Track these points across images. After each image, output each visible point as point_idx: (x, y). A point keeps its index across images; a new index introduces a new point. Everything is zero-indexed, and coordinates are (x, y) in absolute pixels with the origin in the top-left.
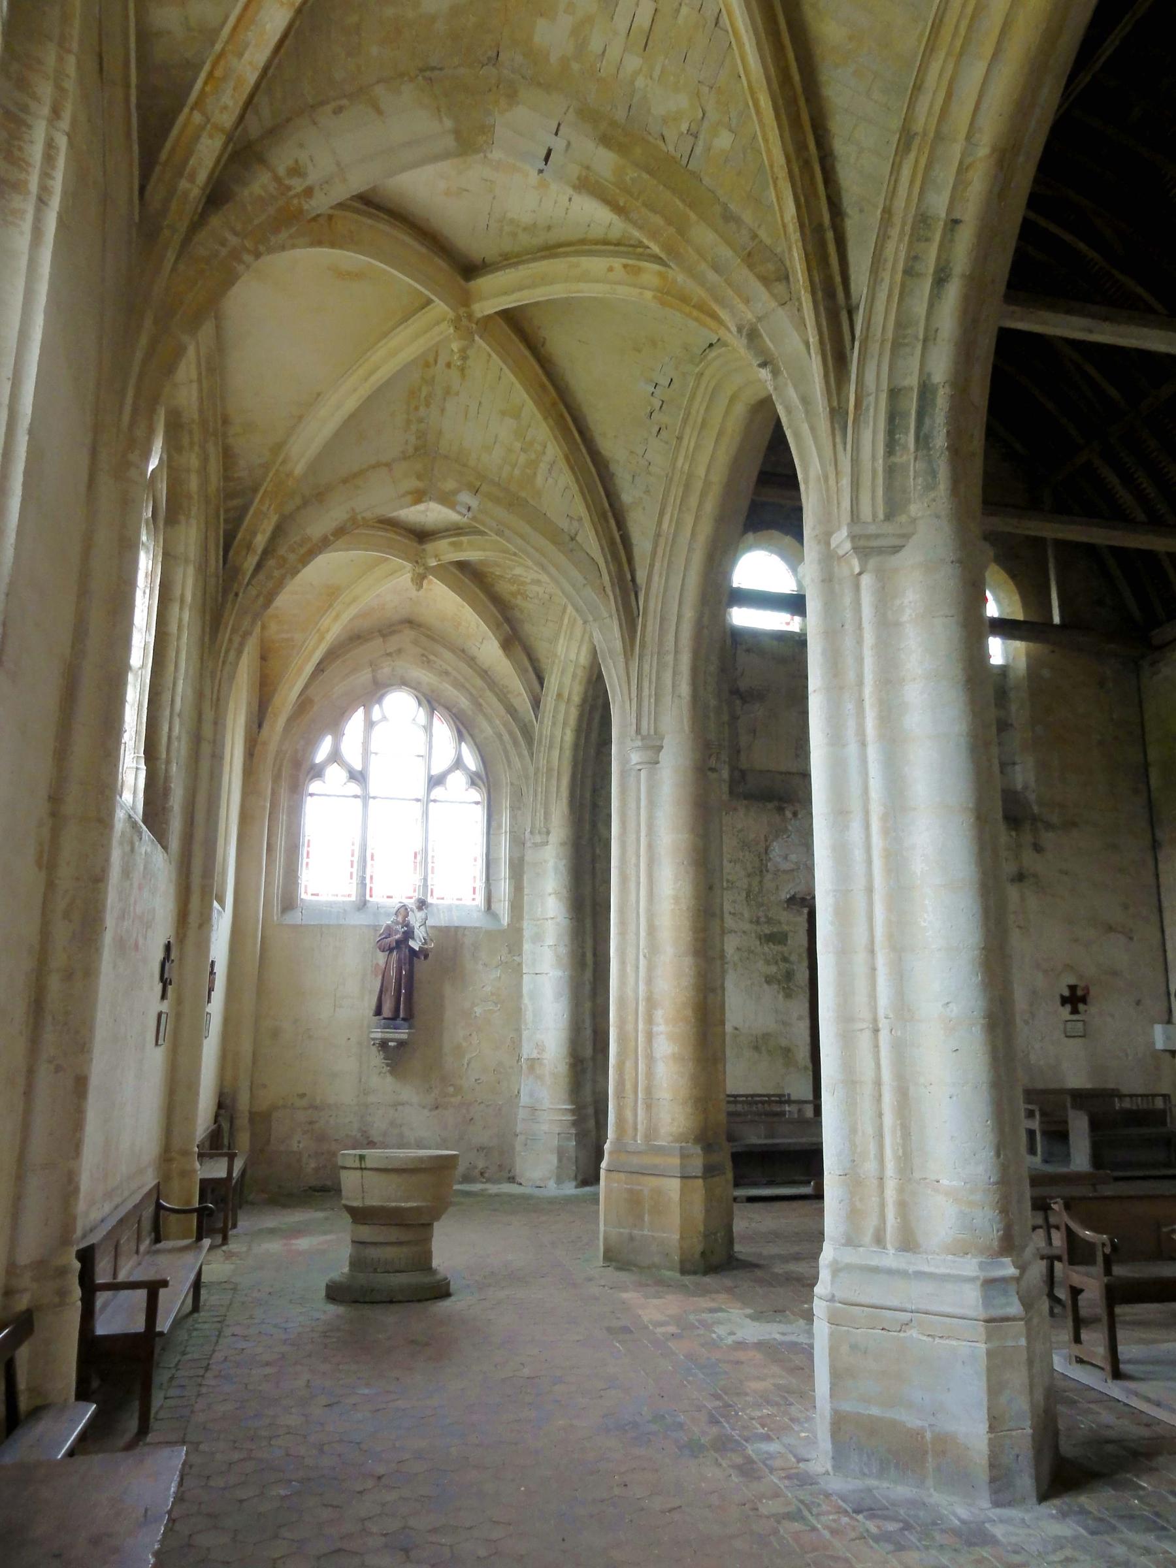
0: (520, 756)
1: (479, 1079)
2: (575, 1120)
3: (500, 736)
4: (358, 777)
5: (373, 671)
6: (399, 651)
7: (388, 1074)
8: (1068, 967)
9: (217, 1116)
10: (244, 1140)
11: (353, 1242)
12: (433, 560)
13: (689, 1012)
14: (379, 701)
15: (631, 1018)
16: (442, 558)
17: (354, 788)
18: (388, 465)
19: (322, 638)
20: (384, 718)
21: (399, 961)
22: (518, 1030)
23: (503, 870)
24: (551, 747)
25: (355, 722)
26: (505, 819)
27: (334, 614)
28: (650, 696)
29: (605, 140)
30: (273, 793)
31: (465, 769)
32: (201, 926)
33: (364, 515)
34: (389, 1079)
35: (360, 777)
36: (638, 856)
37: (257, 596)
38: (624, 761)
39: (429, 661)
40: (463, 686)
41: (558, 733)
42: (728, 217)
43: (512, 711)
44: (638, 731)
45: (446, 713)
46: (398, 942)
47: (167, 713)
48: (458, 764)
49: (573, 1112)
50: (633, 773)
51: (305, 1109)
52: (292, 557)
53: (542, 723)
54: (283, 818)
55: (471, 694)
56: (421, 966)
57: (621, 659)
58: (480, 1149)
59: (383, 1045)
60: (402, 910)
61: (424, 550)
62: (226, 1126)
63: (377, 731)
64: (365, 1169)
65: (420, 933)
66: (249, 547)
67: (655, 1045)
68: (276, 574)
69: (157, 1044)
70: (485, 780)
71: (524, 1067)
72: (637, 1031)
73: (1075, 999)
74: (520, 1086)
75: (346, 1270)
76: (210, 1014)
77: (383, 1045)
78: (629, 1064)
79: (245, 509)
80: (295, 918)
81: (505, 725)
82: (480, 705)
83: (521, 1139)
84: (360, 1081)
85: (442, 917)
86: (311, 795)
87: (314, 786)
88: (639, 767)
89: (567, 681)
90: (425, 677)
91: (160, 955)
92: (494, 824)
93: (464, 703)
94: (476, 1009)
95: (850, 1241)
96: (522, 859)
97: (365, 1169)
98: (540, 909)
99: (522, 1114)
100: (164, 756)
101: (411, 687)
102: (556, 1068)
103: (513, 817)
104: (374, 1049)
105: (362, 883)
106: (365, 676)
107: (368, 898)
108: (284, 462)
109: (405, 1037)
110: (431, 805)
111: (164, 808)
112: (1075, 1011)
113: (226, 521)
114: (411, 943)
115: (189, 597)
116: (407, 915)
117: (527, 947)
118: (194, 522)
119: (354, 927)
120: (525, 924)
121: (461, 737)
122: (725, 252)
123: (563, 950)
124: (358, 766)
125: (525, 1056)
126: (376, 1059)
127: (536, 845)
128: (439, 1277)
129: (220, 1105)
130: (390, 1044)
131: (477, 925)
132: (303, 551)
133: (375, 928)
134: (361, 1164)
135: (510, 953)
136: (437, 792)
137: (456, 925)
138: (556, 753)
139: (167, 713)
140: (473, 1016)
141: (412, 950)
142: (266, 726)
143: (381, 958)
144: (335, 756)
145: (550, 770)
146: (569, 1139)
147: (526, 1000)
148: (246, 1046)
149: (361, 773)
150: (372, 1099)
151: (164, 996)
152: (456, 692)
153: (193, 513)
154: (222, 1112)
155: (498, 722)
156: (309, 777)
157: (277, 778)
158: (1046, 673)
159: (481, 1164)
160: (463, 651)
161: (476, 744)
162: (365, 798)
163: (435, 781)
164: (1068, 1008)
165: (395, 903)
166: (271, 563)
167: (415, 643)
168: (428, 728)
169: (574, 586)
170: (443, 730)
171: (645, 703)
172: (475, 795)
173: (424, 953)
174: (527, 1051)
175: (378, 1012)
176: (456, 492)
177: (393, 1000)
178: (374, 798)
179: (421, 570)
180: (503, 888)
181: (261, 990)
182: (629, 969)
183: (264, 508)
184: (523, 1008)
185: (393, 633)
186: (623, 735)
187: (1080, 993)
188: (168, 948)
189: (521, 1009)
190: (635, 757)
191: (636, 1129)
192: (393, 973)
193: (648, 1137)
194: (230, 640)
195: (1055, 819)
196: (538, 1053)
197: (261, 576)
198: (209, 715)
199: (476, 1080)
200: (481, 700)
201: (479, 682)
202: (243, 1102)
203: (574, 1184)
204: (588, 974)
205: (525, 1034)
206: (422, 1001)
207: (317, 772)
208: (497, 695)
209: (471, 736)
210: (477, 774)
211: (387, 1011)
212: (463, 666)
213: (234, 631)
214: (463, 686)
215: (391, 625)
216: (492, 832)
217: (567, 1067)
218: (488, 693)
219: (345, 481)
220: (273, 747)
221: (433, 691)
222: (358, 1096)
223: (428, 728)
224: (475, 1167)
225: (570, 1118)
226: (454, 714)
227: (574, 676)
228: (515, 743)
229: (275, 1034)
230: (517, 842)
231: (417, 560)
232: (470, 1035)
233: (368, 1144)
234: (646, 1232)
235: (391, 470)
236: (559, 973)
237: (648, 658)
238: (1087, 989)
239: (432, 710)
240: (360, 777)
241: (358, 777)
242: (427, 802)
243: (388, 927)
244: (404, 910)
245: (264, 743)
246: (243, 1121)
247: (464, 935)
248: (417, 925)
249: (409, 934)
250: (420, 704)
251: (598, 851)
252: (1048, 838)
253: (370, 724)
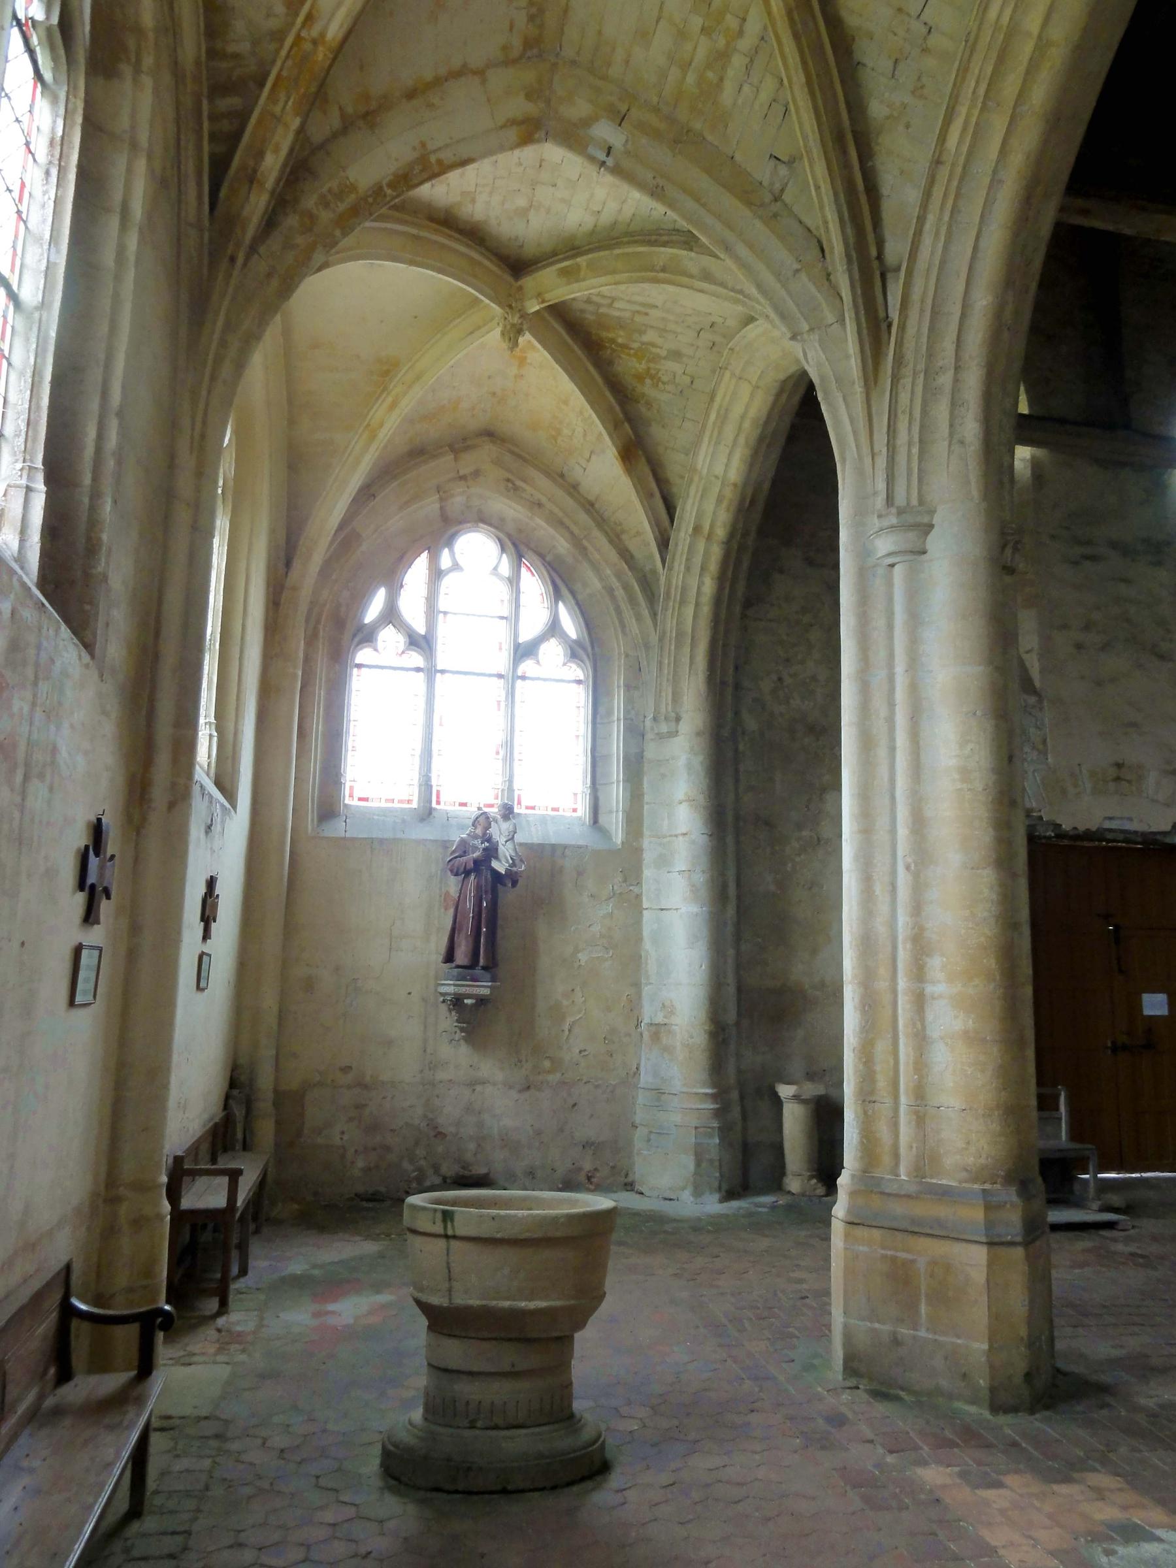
0: (639, 618)
1: (585, 1050)
2: (718, 1109)
3: (610, 591)
4: (421, 643)
5: (441, 499)
6: (477, 473)
7: (462, 1042)
9: (227, 1097)
10: (266, 1131)
11: (429, 1365)
12: (534, 301)
13: (991, 962)
14: (450, 543)
15: (883, 972)
16: (547, 296)
17: (416, 659)
18: (480, 73)
19: (373, 437)
20: (456, 567)
21: (478, 888)
22: (637, 985)
23: (616, 770)
24: (683, 602)
25: (418, 571)
26: (618, 702)
27: (390, 399)
28: (910, 444)
30: (307, 659)
31: (563, 636)
32: (171, 805)
33: (441, 155)
34: (464, 1049)
35: (424, 644)
36: (891, 705)
37: (269, 275)
38: (863, 553)
39: (516, 488)
40: (562, 523)
41: (693, 583)
43: (626, 555)
44: (890, 500)
45: (535, 558)
47: (94, 405)
48: (554, 629)
49: (714, 1097)
50: (881, 571)
51: (349, 1087)
52: (325, 216)
53: (671, 569)
54: (320, 693)
55: (572, 533)
56: (508, 897)
57: (859, 388)
59: (457, 1002)
60: (482, 819)
61: (520, 288)
62: (239, 1112)
63: (447, 582)
64: (454, 1237)
66: (251, 178)
67: (930, 1016)
68: (300, 240)
69: (72, 1003)
70: (589, 649)
71: (646, 1035)
72: (894, 992)
74: (640, 1060)
75: (417, 1415)
76: (210, 956)
77: (457, 1002)
78: (881, 1048)
79: (242, 117)
80: (337, 829)
81: (619, 575)
82: (585, 548)
83: (639, 1134)
84: (425, 1051)
85: (533, 829)
86: (359, 666)
87: (363, 655)
88: (890, 560)
89: (709, 506)
91: (79, 838)
92: (602, 710)
93: (562, 545)
94: (580, 955)
96: (640, 757)
97: (454, 1237)
98: (666, 822)
99: (641, 1098)
100: (87, 480)
101: (490, 525)
102: (692, 1037)
103: (629, 701)
104: (443, 1008)
106: (430, 506)
107: (434, 805)
108: (310, 18)
109: (487, 992)
110: (519, 683)
111: (87, 575)
113: (213, 137)
114: (495, 864)
115: (138, 209)
116: (489, 826)
117: (647, 873)
118: (147, 82)
119: (419, 842)
120: (646, 843)
121: (557, 595)
123: (700, 878)
124: (420, 628)
125: (646, 1020)
126: (447, 1021)
127: (660, 736)
128: (587, 1435)
129: (233, 1083)
130: (466, 1001)
131: (581, 842)
132: (342, 207)
133: (445, 844)
134: (445, 1228)
135: (625, 881)
136: (527, 667)
137: (553, 842)
138: (689, 611)
139: (94, 405)
140: (576, 965)
141: (495, 873)
142: (297, 564)
143: (453, 885)
144: (391, 615)
145: (680, 635)
146: (711, 1136)
147: (647, 945)
148: (269, 1001)
149: (425, 637)
150: (441, 1075)
151: (90, 916)
152: (551, 531)
153: (148, 61)
154: (235, 1092)
155: (608, 572)
156: (356, 640)
157: (311, 640)
159: (587, 1166)
160: (562, 476)
161: (577, 603)
162: (431, 672)
163: (524, 651)
165: (472, 811)
166: (291, 221)
167: (498, 462)
168: (514, 582)
169: (777, 275)
170: (533, 585)
171: (901, 458)
172: (576, 671)
173: (512, 878)
174: (649, 1013)
175: (449, 957)
176: (587, 122)
177: (470, 940)
178: (443, 672)
179: (516, 319)
180: (616, 794)
181: (290, 928)
182: (878, 889)
183: (277, 109)
184: (643, 954)
185: (467, 448)
186: (860, 513)
188: (97, 831)
189: (641, 957)
190: (884, 545)
191: (896, 1156)
192: (469, 905)
193: (918, 1171)
194: (223, 343)
196: (665, 1017)
197: (274, 243)
198: (186, 459)
199: (580, 1052)
200: (585, 543)
201: (583, 517)
202: (265, 1081)
203: (716, 1196)
204: (731, 911)
205: (646, 991)
206: (508, 942)
207: (367, 636)
208: (606, 534)
209: (573, 593)
211: (461, 956)
212: (560, 494)
213: (228, 327)
214: (562, 523)
215: (464, 439)
216: (598, 720)
217: (706, 1036)
218: (597, 533)
219: (411, 95)
221: (520, 531)
222: (422, 1071)
223: (514, 582)
224: (580, 1169)
225: (712, 1106)
226: (549, 564)
227: (719, 500)
228: (632, 600)
229: (309, 985)
230: (635, 732)
231: (510, 301)
232: (573, 990)
233: (435, 1136)
234: (922, 1333)
235: (484, 82)
236: (694, 909)
237: (907, 382)
239: (518, 557)
240: (424, 644)
241: (421, 643)
242: (511, 678)
243: (463, 842)
244: (483, 820)
245: (294, 589)
246: (265, 1105)
247: (563, 855)
248: (502, 840)
249: (491, 852)
250: (503, 549)
251: (741, 747)
253: (436, 575)
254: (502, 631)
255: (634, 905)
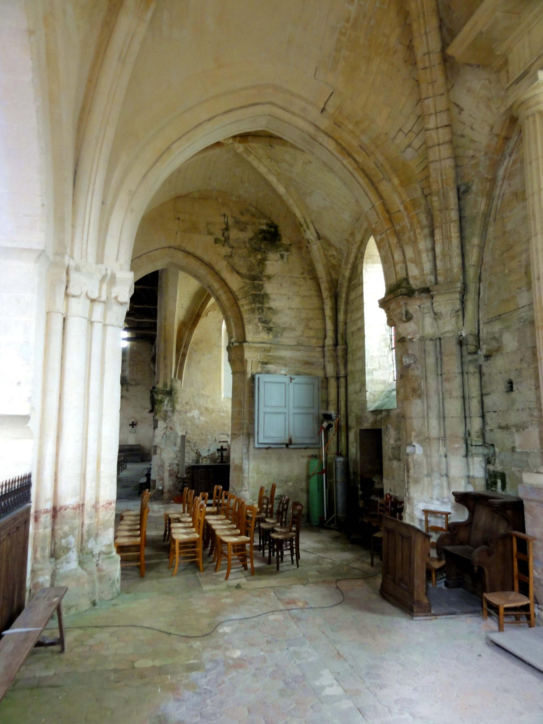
8: (133, 418)
73: (133, 425)
112: (133, 427)
158: (135, 348)
164: (131, 427)
187: (135, 423)
195: (133, 383)
238: (137, 422)
252: (130, 388)
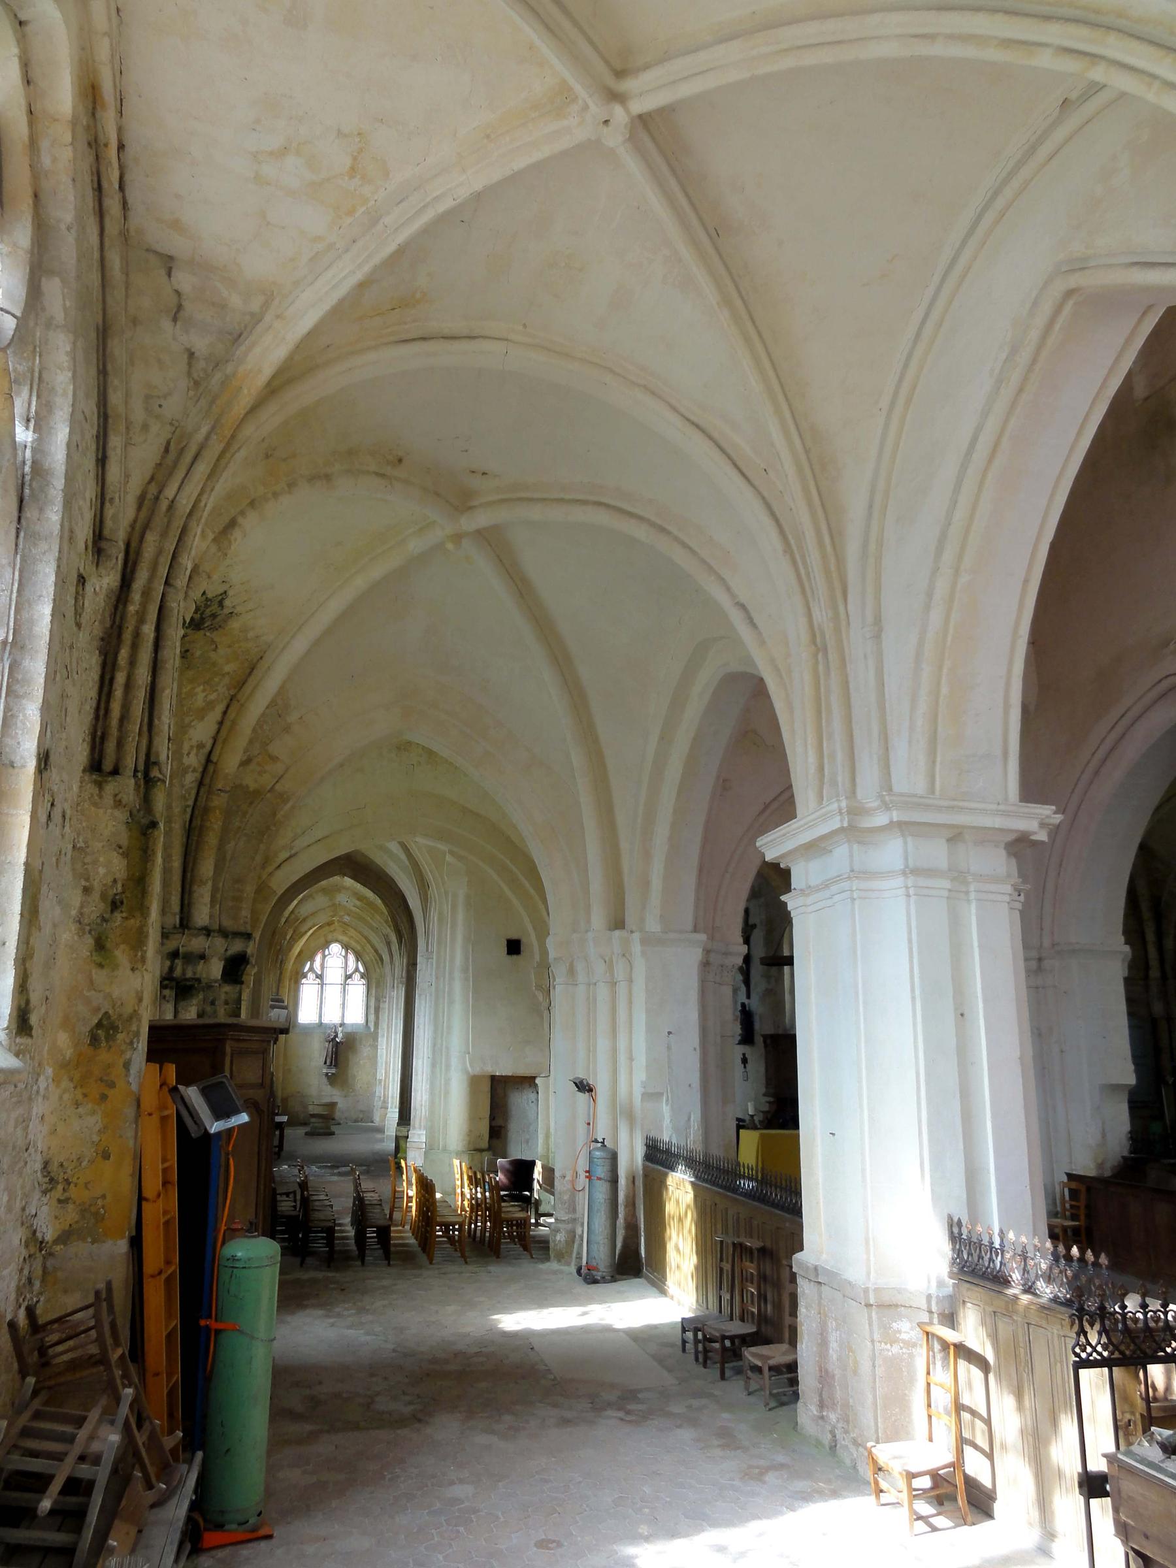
4: (320, 977)
6: (335, 930)
14: (328, 948)
17: (318, 981)
20: (329, 954)
23: (372, 1011)
29: (358, 899)
31: (360, 972)
34: (329, 1087)
42: (382, 913)
46: (332, 1039)
48: (357, 970)
58: (361, 1111)
65: (340, 1035)
77: (327, 1074)
87: (304, 981)
90: (345, 939)
93: (359, 948)
95: (391, 1108)
96: (379, 1007)
99: (376, 1099)
103: (376, 991)
105: (320, 1016)
121: (357, 960)
122: (382, 921)
124: (320, 973)
126: (325, 1080)
136: (349, 981)
143: (327, 1044)
144: (311, 969)
149: (321, 975)
150: (323, 1094)
159: (361, 1116)
162: (322, 984)
163: (348, 977)
168: (346, 957)
170: (351, 958)
175: (325, 1063)
180: (372, 1017)
192: (330, 1050)
207: (305, 976)
210: (363, 973)
211: (328, 1063)
220: (289, 970)
223: (346, 957)
228: (377, 963)
230: (378, 1000)
241: (320, 977)
254: (341, 971)
255: (376, 1047)
